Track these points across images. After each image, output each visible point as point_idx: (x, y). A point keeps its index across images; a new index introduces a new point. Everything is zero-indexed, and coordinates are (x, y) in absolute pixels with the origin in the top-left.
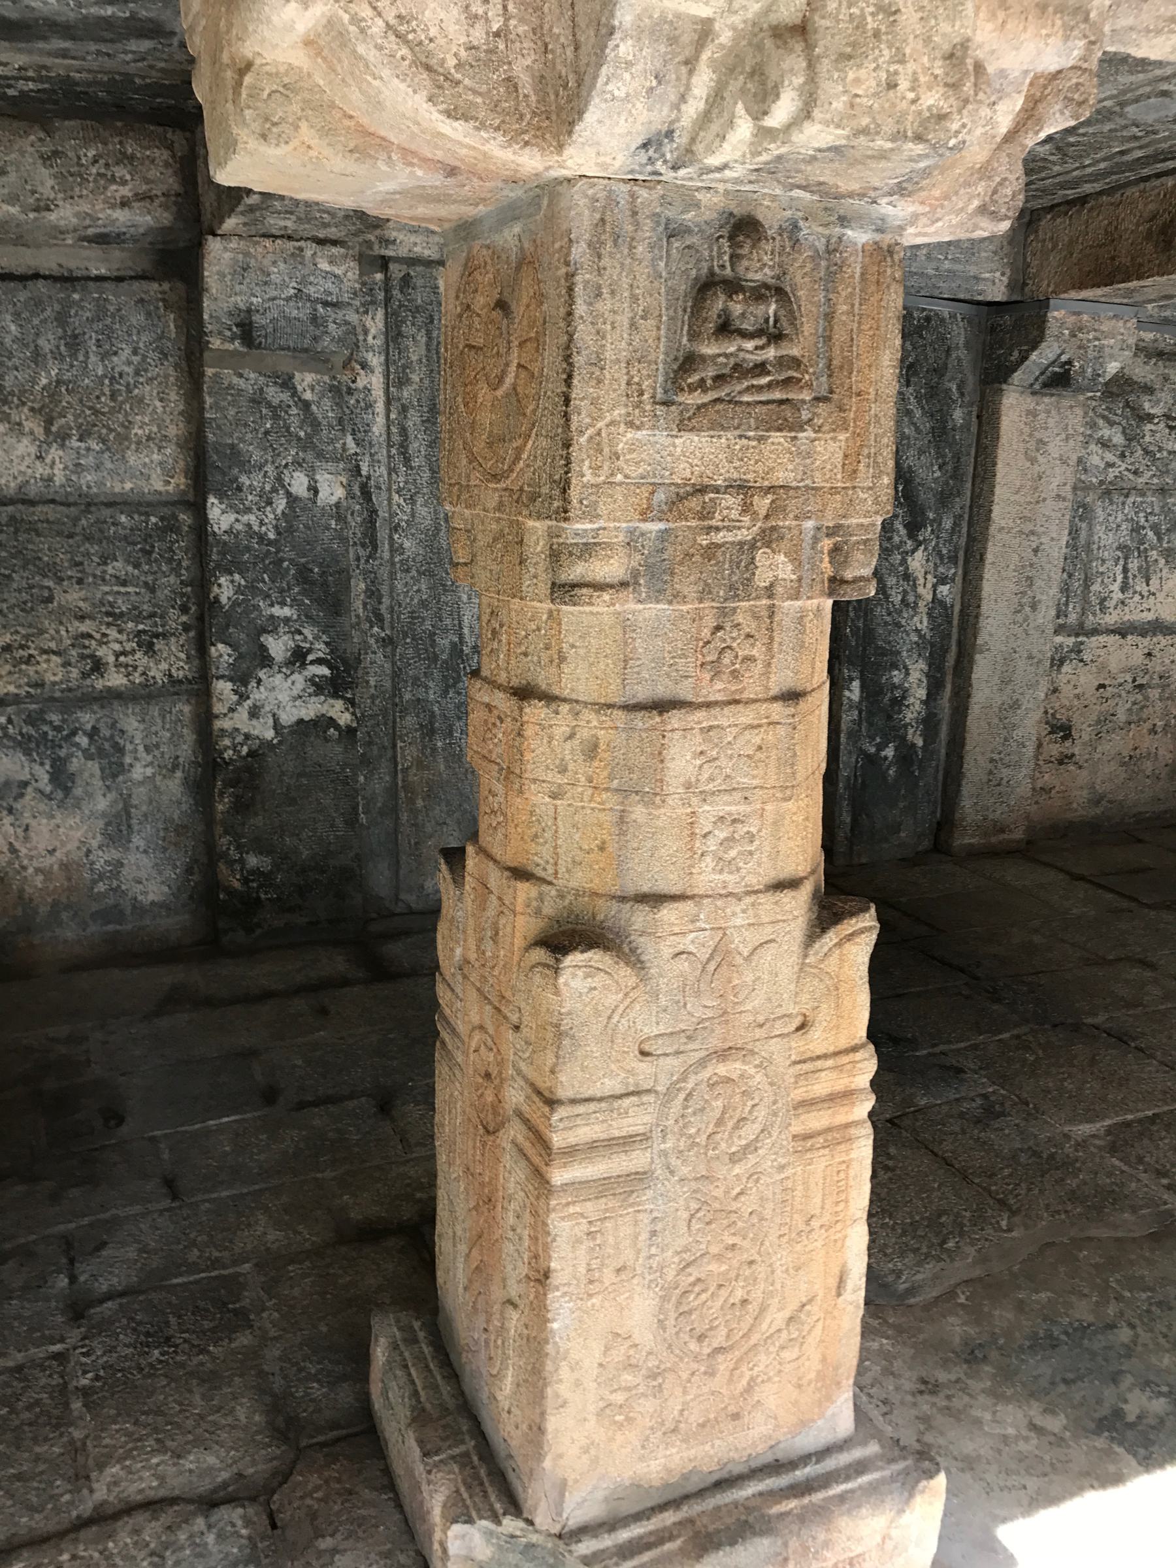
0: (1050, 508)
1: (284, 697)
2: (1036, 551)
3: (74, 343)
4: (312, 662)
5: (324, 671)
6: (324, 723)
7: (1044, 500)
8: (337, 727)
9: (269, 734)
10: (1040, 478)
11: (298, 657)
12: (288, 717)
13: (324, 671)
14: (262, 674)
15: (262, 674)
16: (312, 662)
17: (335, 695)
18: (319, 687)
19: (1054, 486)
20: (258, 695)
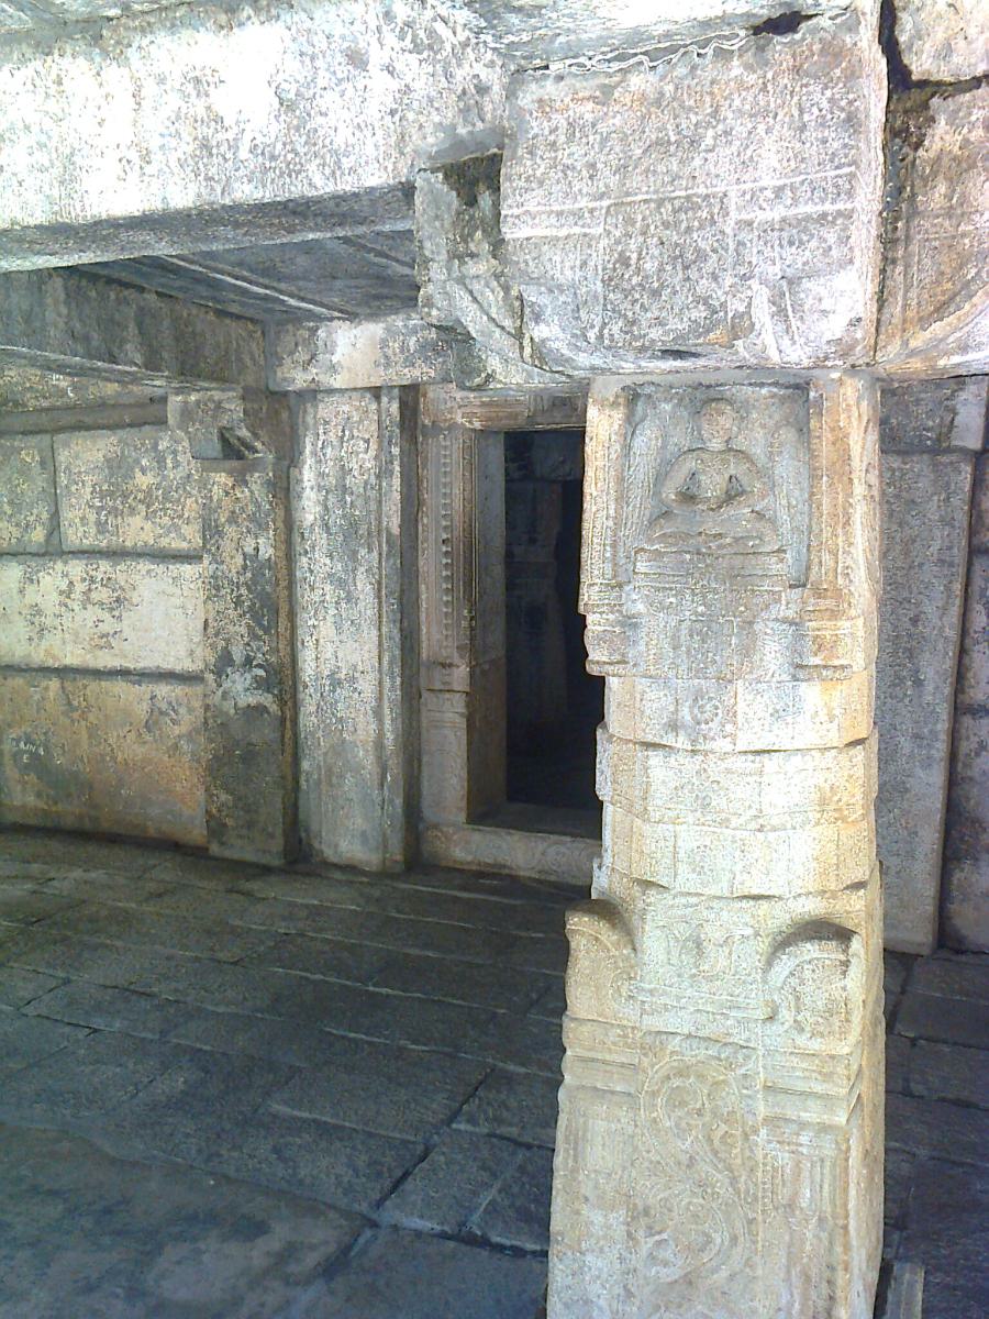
0: (929, 572)
1: (240, 687)
2: (915, 621)
3: (161, 461)
4: (256, 666)
5: (264, 674)
6: (260, 709)
7: (921, 565)
8: (268, 713)
9: (232, 711)
10: (914, 541)
11: (248, 662)
12: (242, 703)
13: (261, 673)
14: (229, 670)
15: (229, 670)
16: (256, 666)
17: (268, 691)
18: (261, 685)
19: (936, 546)
20: (227, 684)
